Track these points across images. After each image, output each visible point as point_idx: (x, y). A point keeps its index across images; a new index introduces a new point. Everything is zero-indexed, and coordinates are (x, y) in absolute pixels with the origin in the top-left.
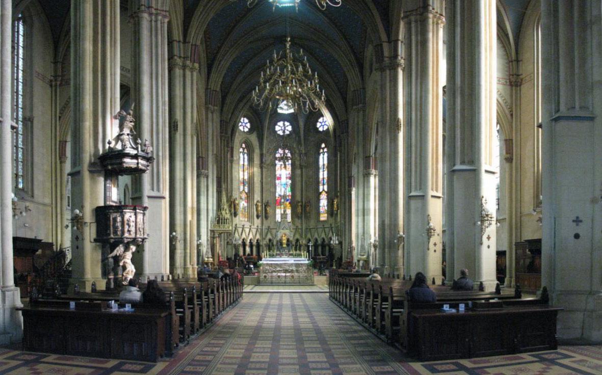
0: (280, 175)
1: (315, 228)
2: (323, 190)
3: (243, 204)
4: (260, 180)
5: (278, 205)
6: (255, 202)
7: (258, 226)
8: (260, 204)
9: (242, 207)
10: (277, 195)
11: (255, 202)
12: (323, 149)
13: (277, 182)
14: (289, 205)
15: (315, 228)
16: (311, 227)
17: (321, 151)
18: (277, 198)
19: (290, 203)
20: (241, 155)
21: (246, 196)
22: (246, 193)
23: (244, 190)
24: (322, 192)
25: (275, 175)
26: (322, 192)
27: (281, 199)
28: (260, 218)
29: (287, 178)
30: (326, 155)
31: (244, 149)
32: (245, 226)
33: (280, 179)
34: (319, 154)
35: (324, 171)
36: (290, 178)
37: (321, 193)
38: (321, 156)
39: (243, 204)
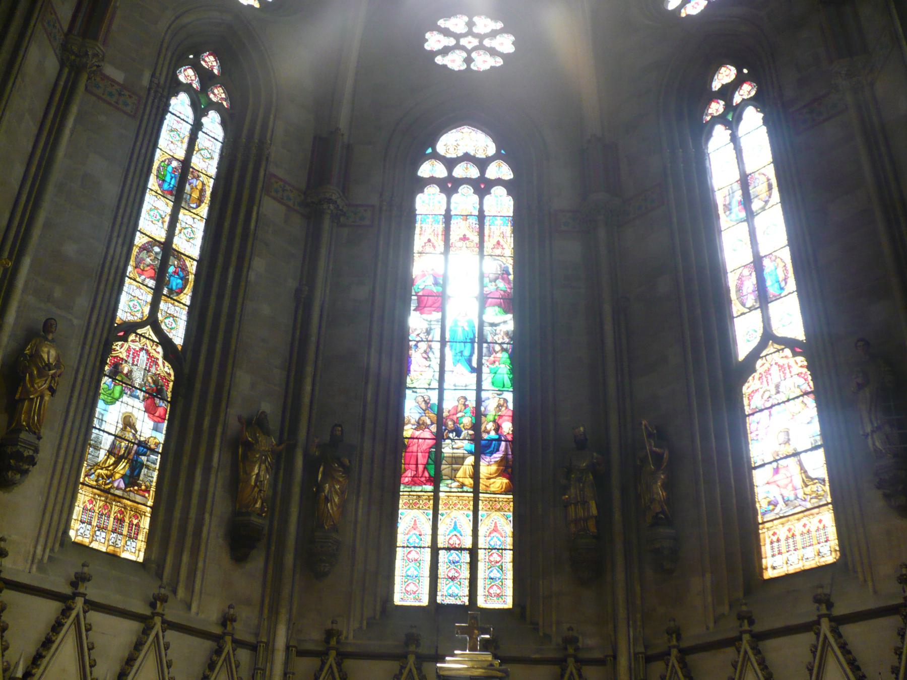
0: (441, 281)
1: (733, 642)
2: (768, 337)
3: (128, 423)
4: (292, 284)
5: (415, 481)
6: (234, 414)
7: (226, 620)
8: (266, 443)
9: (107, 442)
10: (412, 409)
11: (234, 414)
12: (727, 92)
13: (416, 322)
14: (501, 482)
15: (733, 642)
16: (684, 644)
17: (716, 108)
18: (408, 431)
19: (506, 468)
20: (181, 104)
21: (165, 369)
22: (165, 342)
23: (153, 321)
24: (755, 355)
25: (407, 282)
26: (755, 355)
27: (439, 438)
28: (257, 563)
29: (484, 300)
30: (752, 118)
31: (207, 78)
32: (92, 591)
33: (441, 309)
34: (703, 131)
35: (750, 215)
36: (508, 303)
37: (748, 367)
38: (720, 133)
39: (128, 423)
